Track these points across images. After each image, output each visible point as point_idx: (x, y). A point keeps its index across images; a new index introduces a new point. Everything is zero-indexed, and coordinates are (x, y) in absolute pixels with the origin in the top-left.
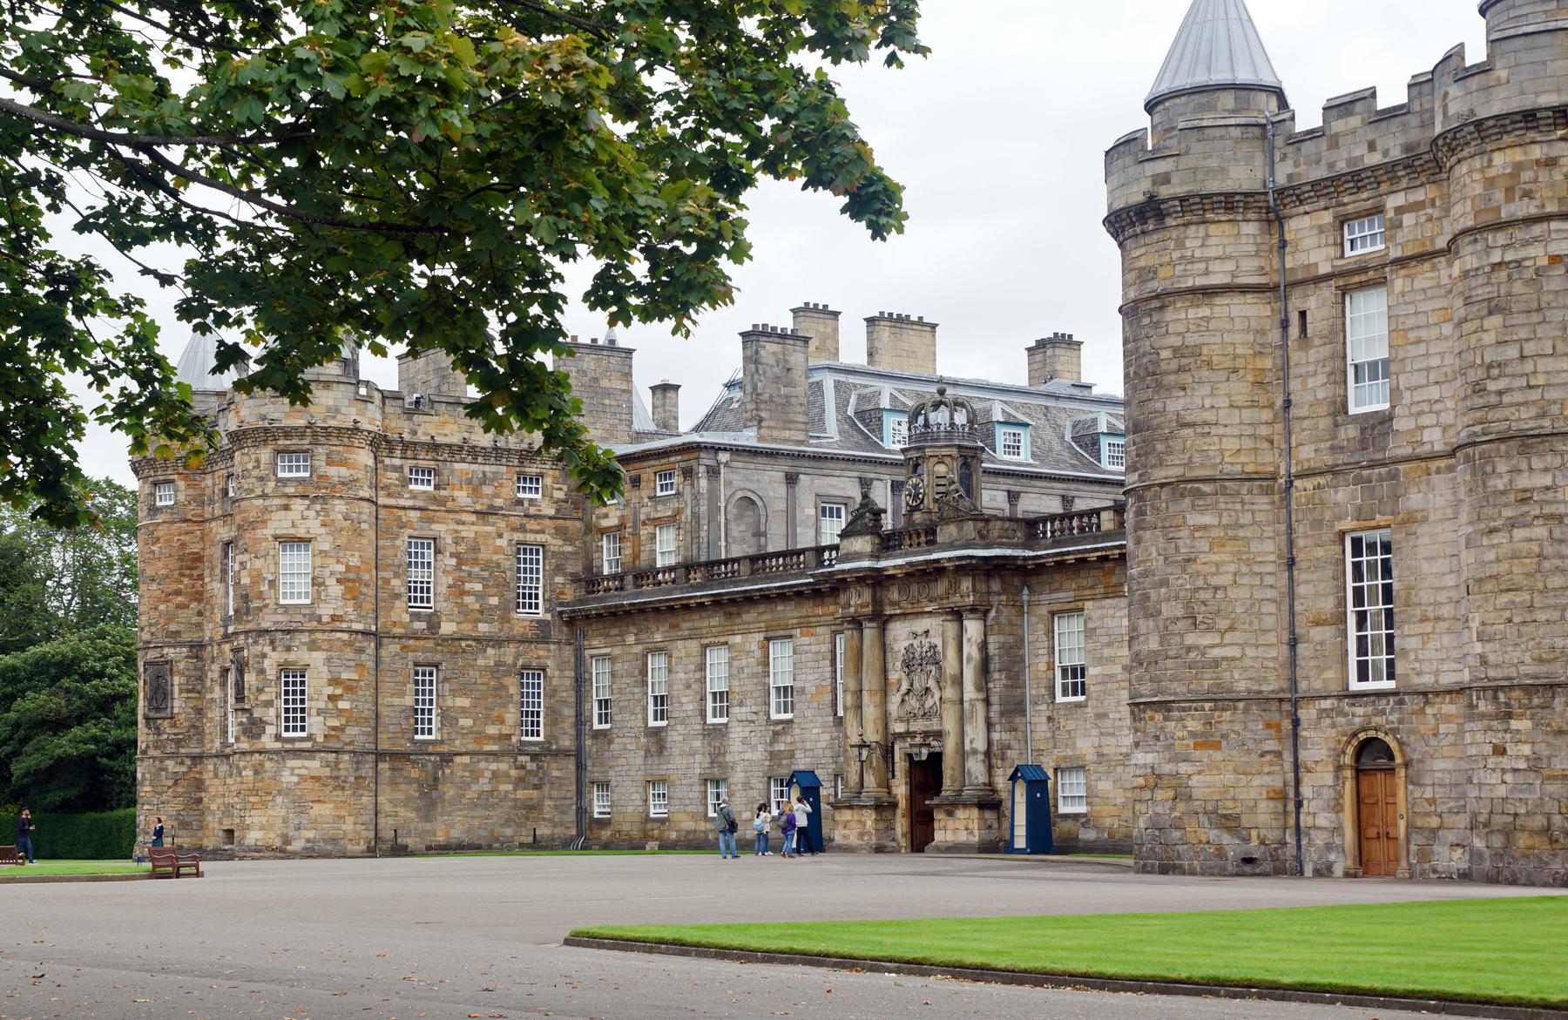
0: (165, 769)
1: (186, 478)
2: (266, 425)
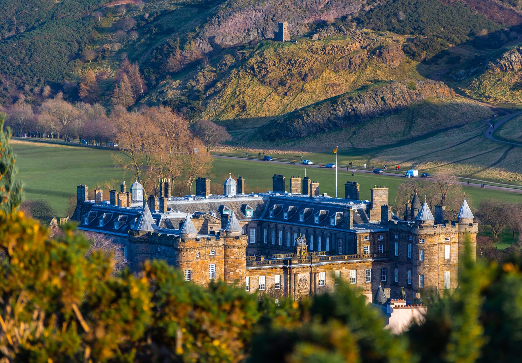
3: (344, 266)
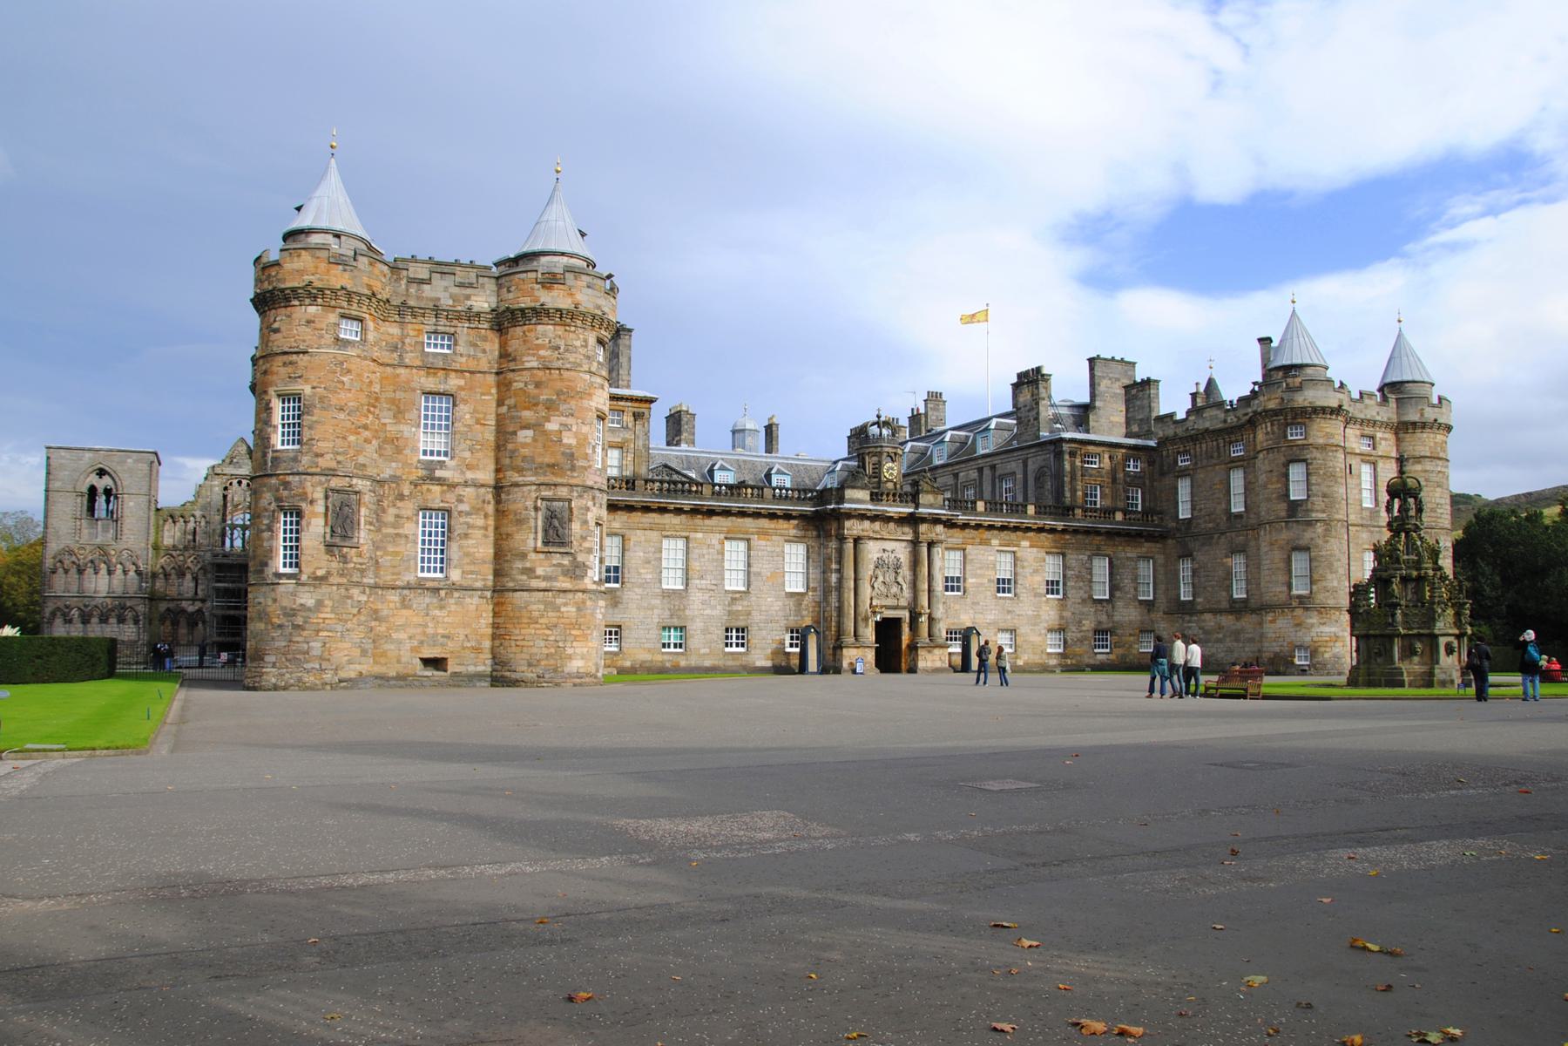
0: (350, 597)
1: (375, 319)
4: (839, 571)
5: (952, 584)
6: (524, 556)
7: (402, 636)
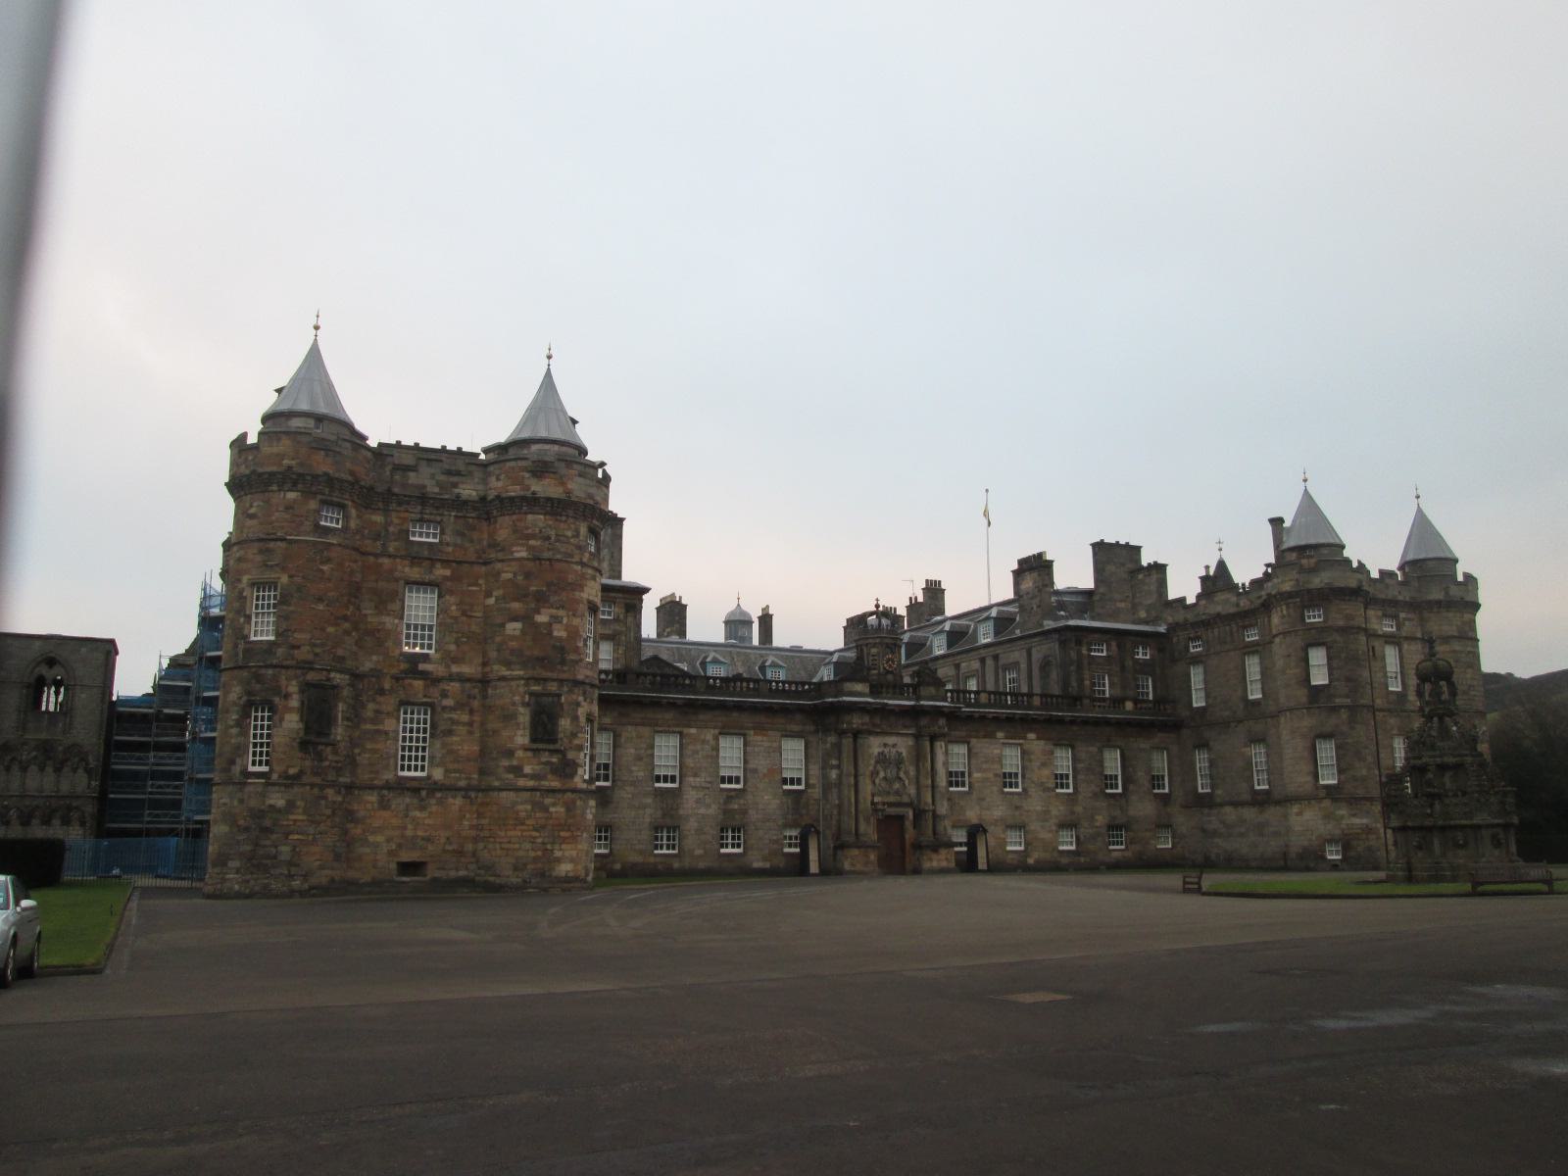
0: (325, 798)
2: (591, 502)
3: (1031, 731)
4: (838, 767)
5: (955, 778)
6: (510, 753)
7: (380, 838)
